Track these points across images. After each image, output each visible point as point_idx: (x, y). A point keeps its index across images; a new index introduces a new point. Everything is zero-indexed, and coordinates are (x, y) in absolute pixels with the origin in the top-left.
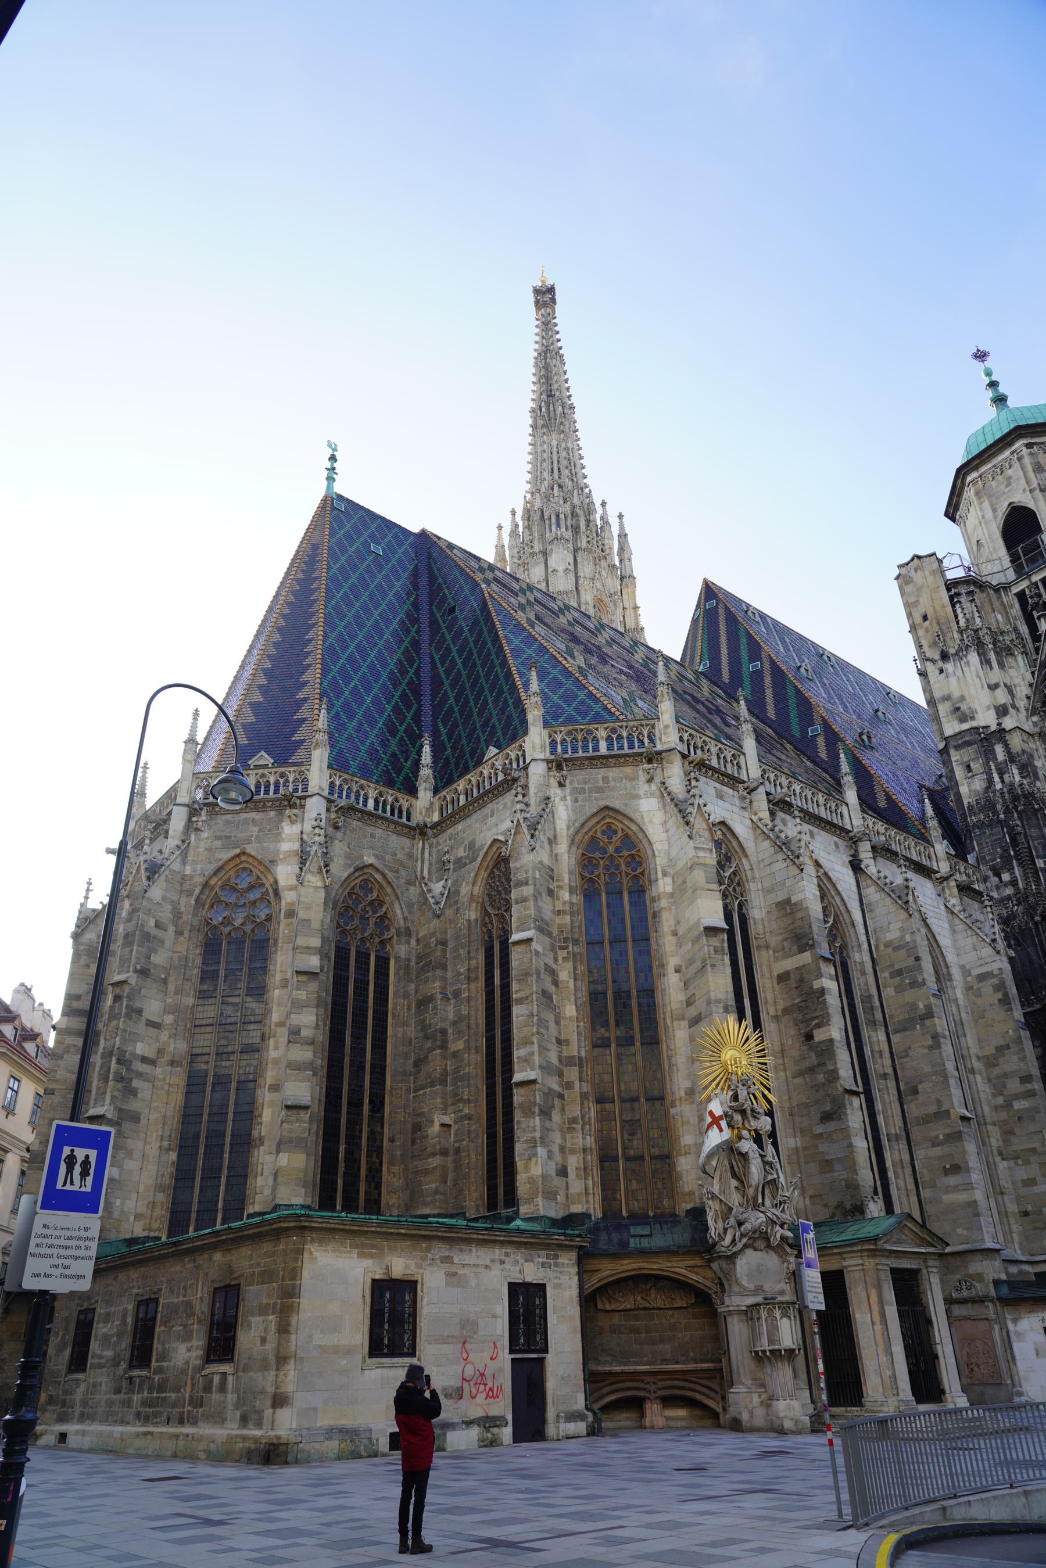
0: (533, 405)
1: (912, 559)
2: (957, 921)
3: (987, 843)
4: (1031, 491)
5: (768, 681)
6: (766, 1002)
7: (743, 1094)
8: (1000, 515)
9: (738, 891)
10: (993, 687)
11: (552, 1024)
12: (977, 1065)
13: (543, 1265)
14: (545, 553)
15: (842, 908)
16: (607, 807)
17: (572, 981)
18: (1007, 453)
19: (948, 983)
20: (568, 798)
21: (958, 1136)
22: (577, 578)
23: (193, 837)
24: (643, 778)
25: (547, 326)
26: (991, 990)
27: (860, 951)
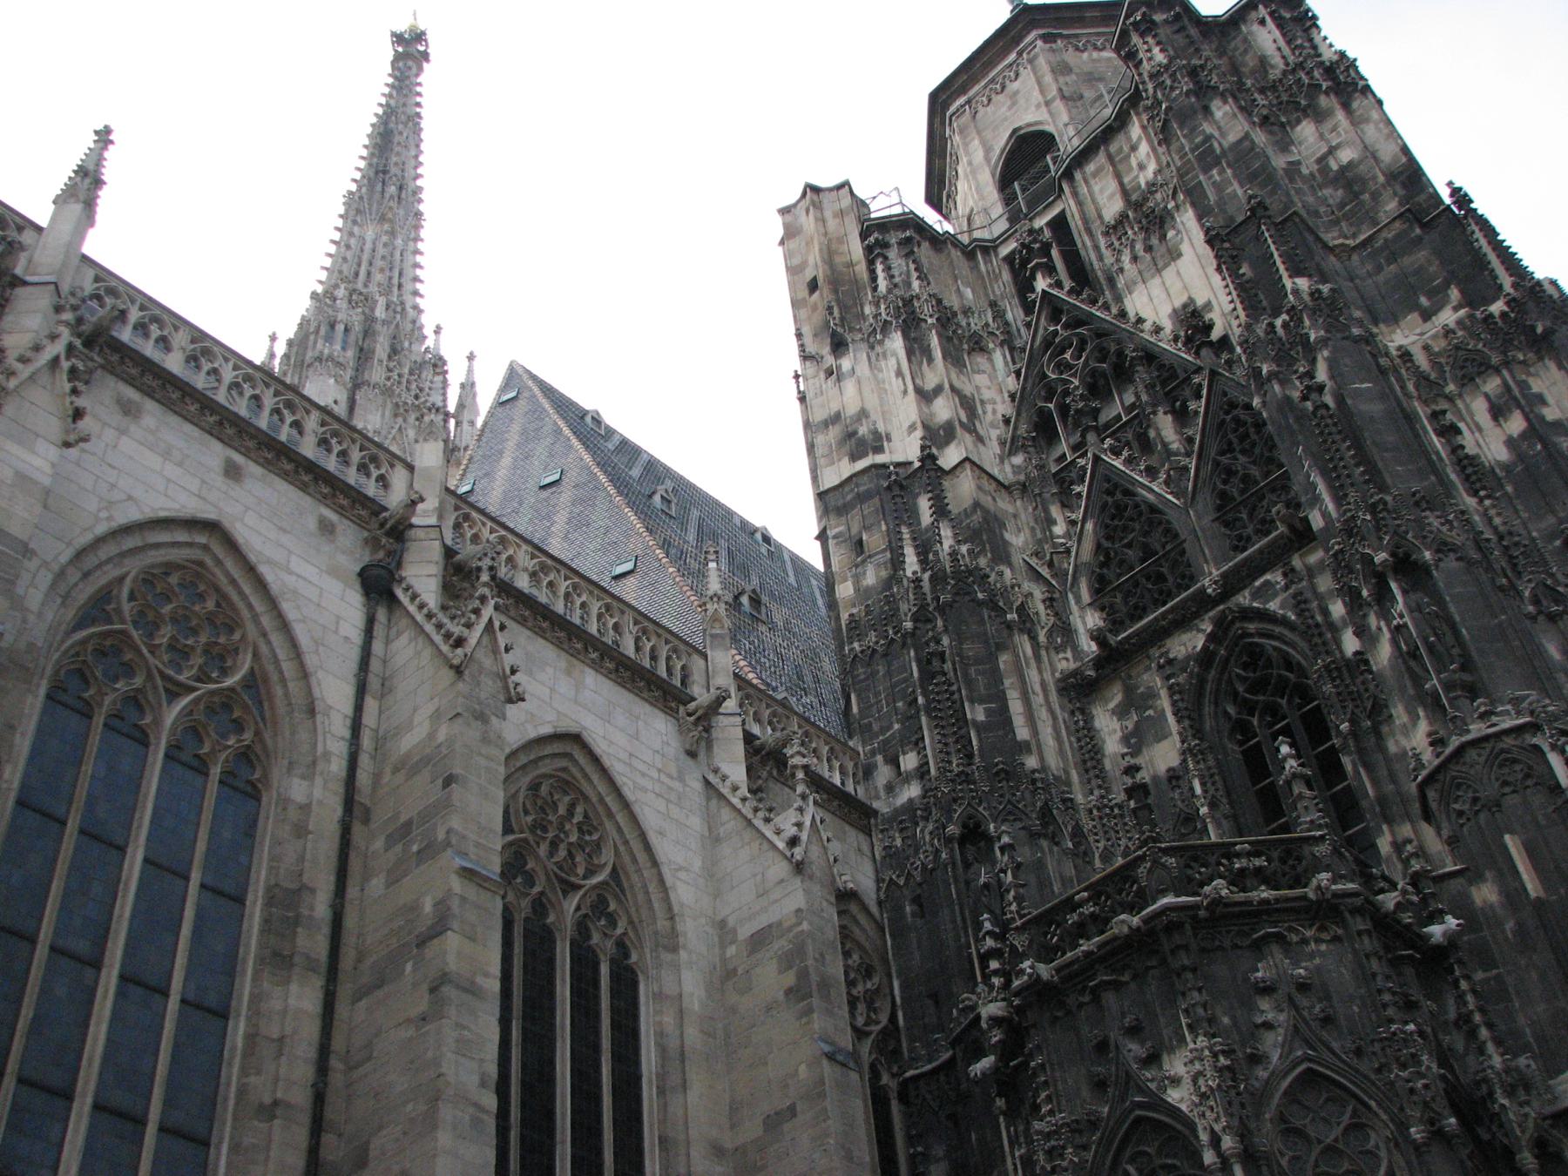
1: (804, 194)
2: (726, 813)
4: (1047, 104)
8: (998, 152)
15: (288, 668)
18: (1013, 56)
19: (666, 957)
27: (309, 776)
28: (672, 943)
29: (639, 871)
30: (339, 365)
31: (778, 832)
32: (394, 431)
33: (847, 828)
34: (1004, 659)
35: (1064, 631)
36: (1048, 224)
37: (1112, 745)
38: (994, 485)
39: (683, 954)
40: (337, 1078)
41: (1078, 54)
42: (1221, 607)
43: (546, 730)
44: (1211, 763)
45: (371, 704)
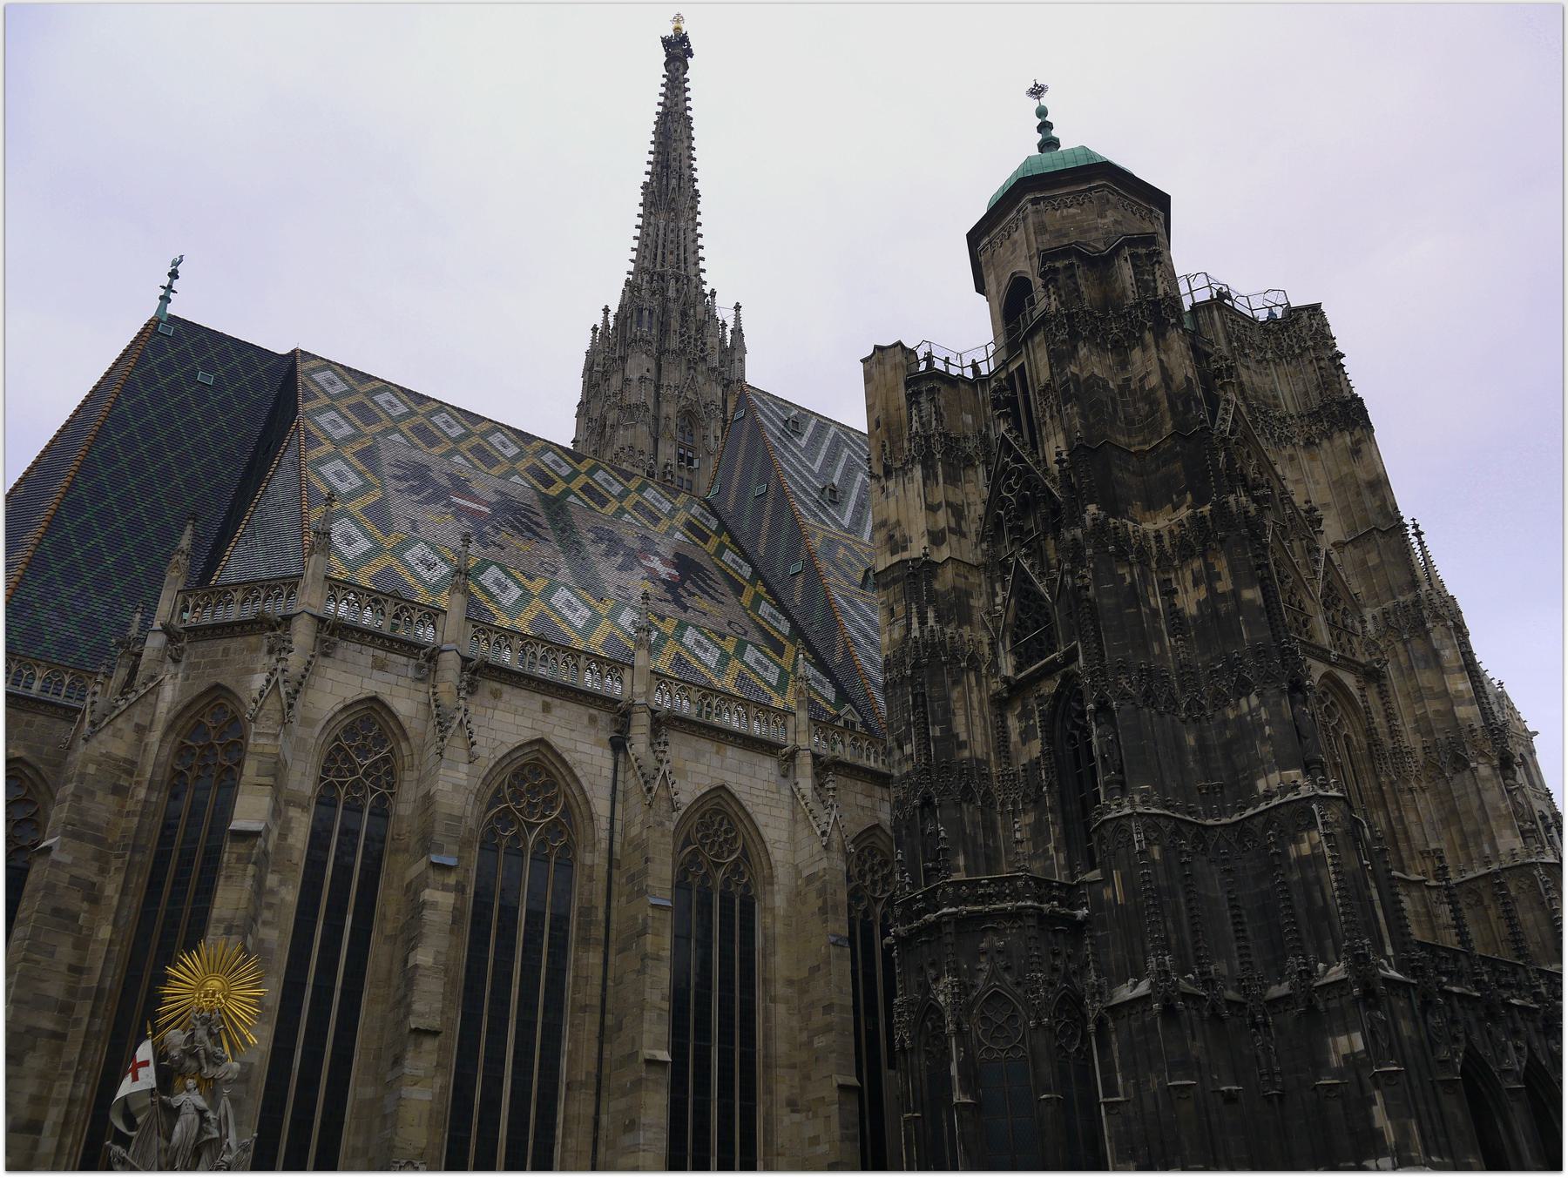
0: (647, 178)
3: (896, 706)
4: (1031, 258)
5: (769, 507)
6: (384, 917)
10: (932, 508)
11: (65, 951)
12: (780, 989)
14: (623, 359)
16: (218, 686)
17: (117, 896)
19: (768, 888)
20: (180, 675)
21: (638, 1084)
22: (658, 387)
24: (265, 649)
26: (814, 894)
27: (592, 852)
28: (770, 880)
29: (756, 846)
33: (876, 787)
34: (955, 694)
35: (994, 664)
37: (1014, 737)
39: (776, 887)
40: (610, 991)
42: (1066, 669)
43: (703, 791)
44: (1053, 760)
45: (619, 807)
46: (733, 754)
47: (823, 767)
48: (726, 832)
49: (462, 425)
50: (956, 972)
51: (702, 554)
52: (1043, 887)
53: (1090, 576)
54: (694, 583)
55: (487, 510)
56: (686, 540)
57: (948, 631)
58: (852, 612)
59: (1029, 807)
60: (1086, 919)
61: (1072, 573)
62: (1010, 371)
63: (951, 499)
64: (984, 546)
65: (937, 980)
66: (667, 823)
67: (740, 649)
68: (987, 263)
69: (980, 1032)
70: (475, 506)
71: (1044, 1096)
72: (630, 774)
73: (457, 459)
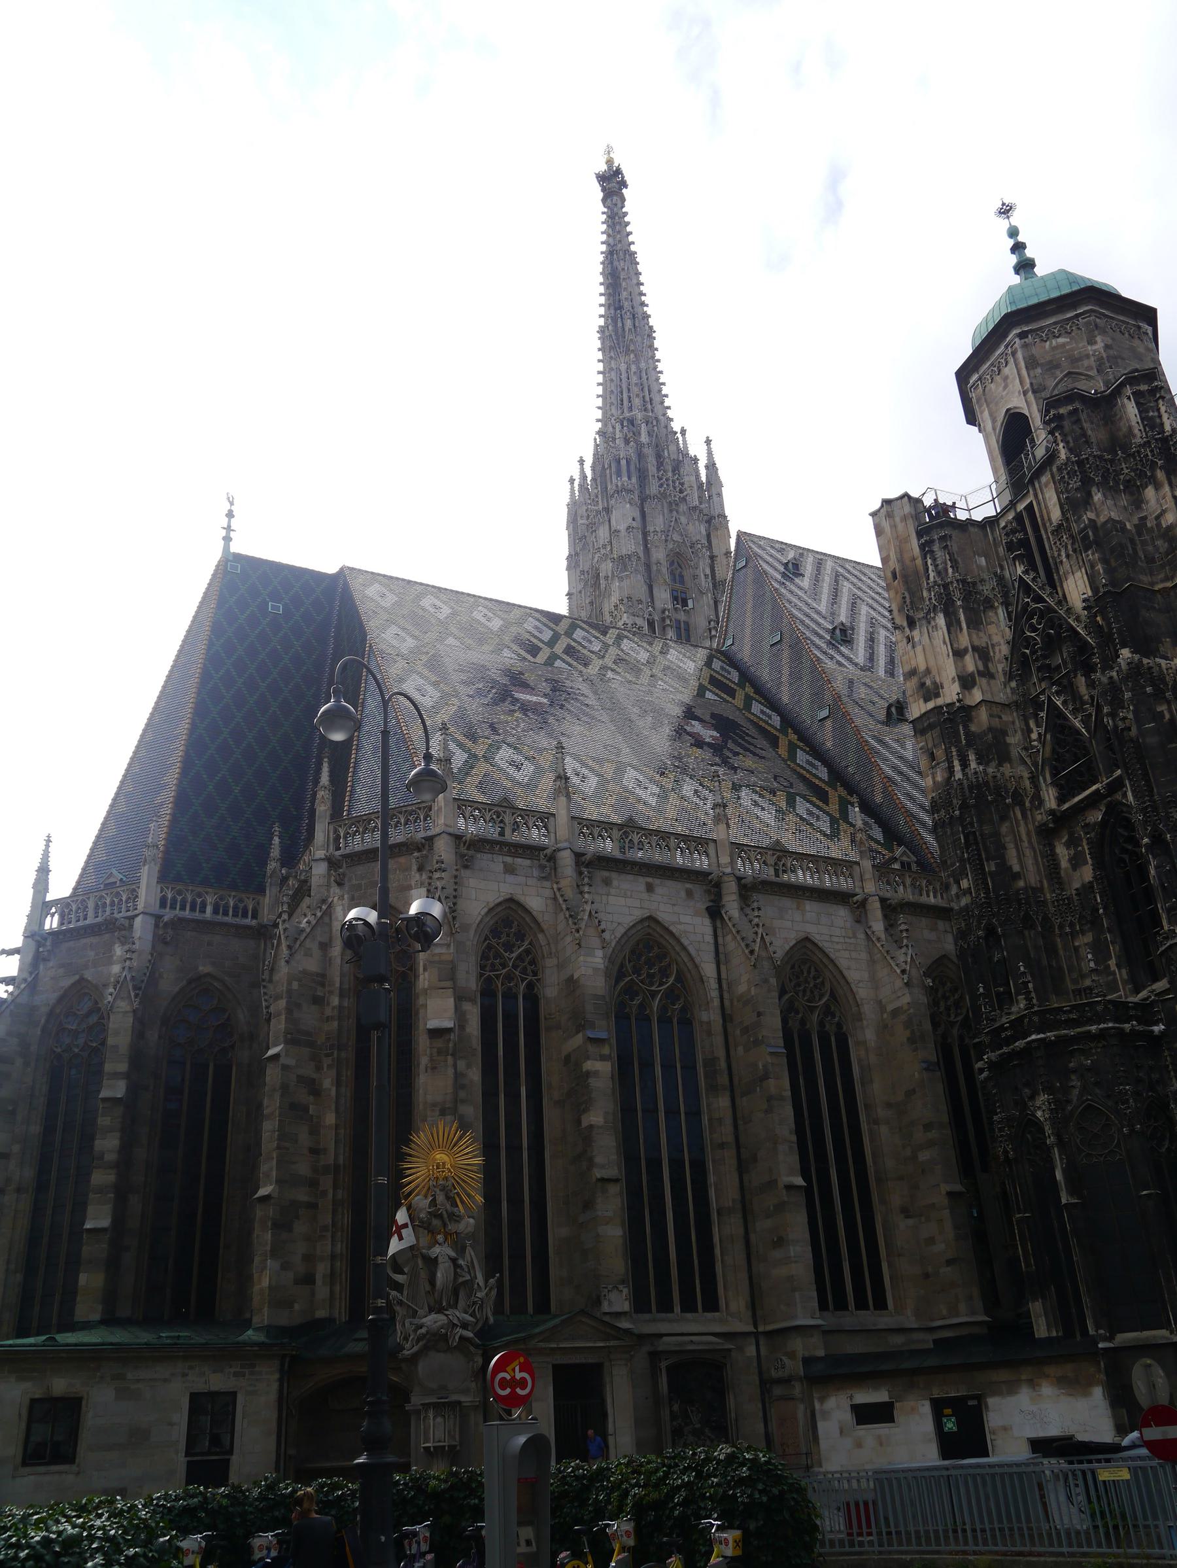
0: (602, 322)
1: (882, 506)
3: (948, 844)
4: (1025, 393)
5: (786, 654)
7: (441, 1198)
9: (529, 971)
10: (959, 654)
13: (236, 1374)
14: (607, 510)
15: (689, 965)
17: (334, 1089)
18: (1002, 347)
20: (346, 896)
22: (645, 534)
23: (41, 967)
24: (415, 867)
25: (616, 221)
28: (859, 1017)
30: (630, 491)
31: (897, 965)
32: (673, 524)
34: (1004, 828)
35: (1038, 799)
36: (1025, 508)
37: (1064, 864)
38: (1000, 706)
39: (865, 1022)
41: (1043, 344)
43: (791, 944)
45: (723, 968)
46: (811, 908)
47: (890, 910)
48: (815, 978)
49: (499, 617)
50: (1049, 1089)
51: (730, 710)
52: (1120, 1010)
53: (1131, 716)
54: (735, 742)
55: (545, 701)
56: (716, 698)
57: (990, 770)
58: (884, 751)
59: (1086, 928)
60: (1162, 1033)
61: (1113, 715)
62: (1018, 510)
63: (976, 643)
64: (1013, 684)
65: (1032, 1097)
66: (771, 980)
67: (791, 802)
68: (978, 400)
69: (1078, 1141)
70: (534, 699)
71: (1145, 1193)
72: (729, 938)
73: (506, 653)
